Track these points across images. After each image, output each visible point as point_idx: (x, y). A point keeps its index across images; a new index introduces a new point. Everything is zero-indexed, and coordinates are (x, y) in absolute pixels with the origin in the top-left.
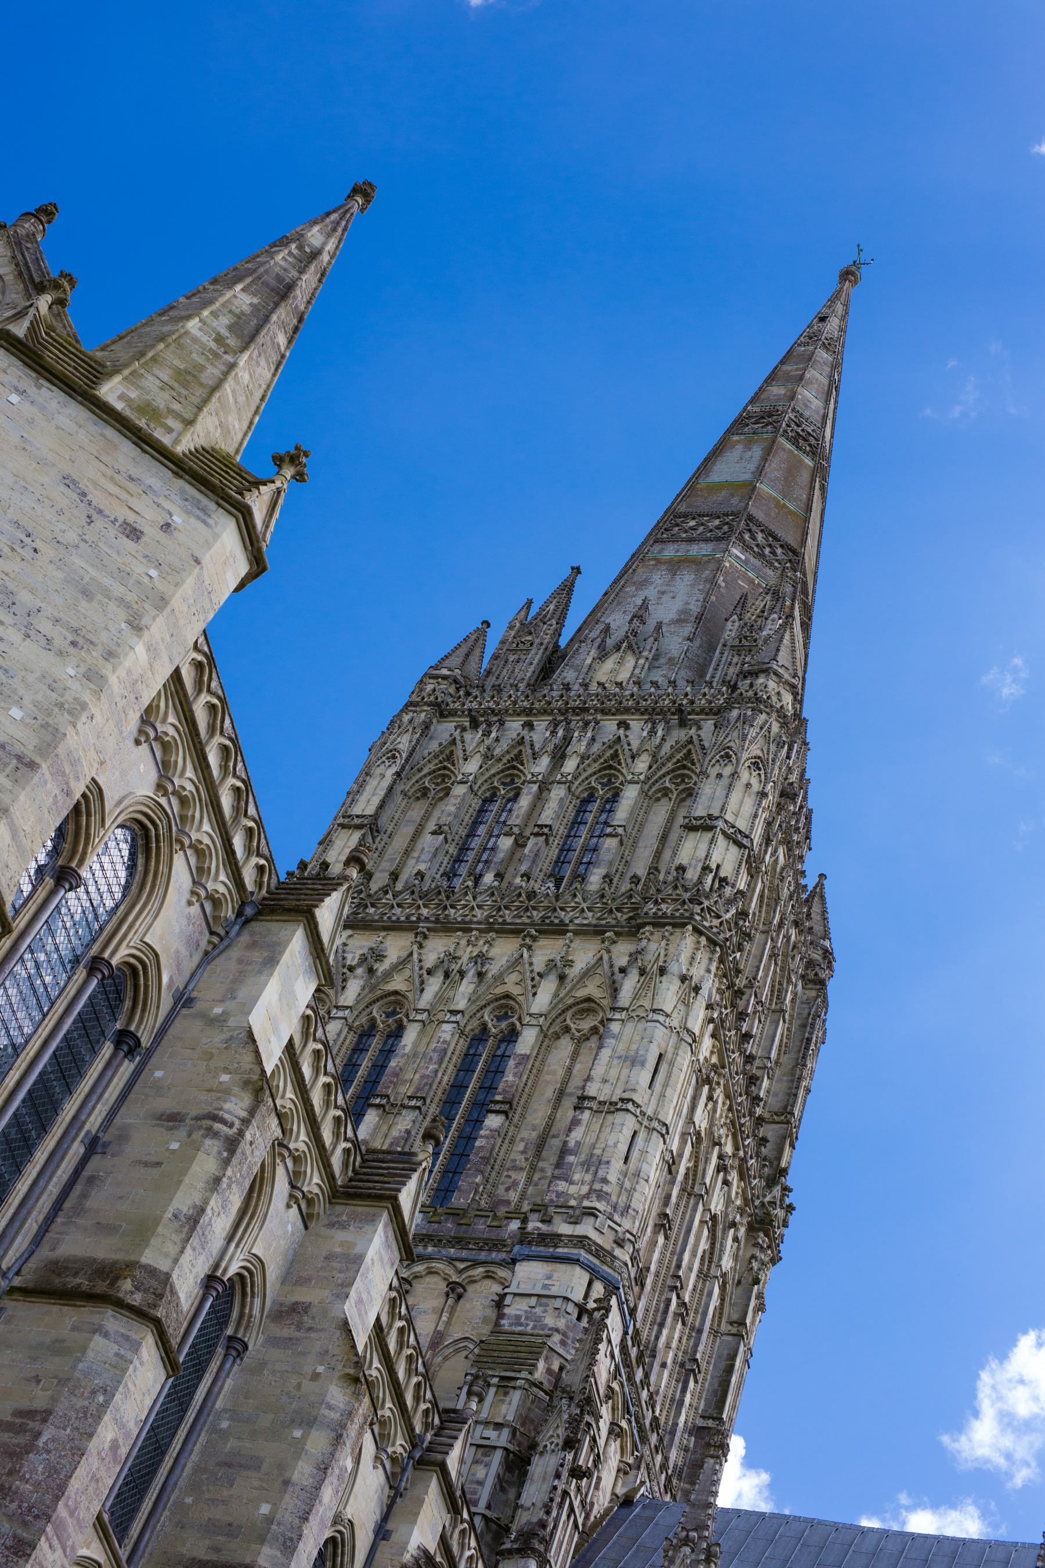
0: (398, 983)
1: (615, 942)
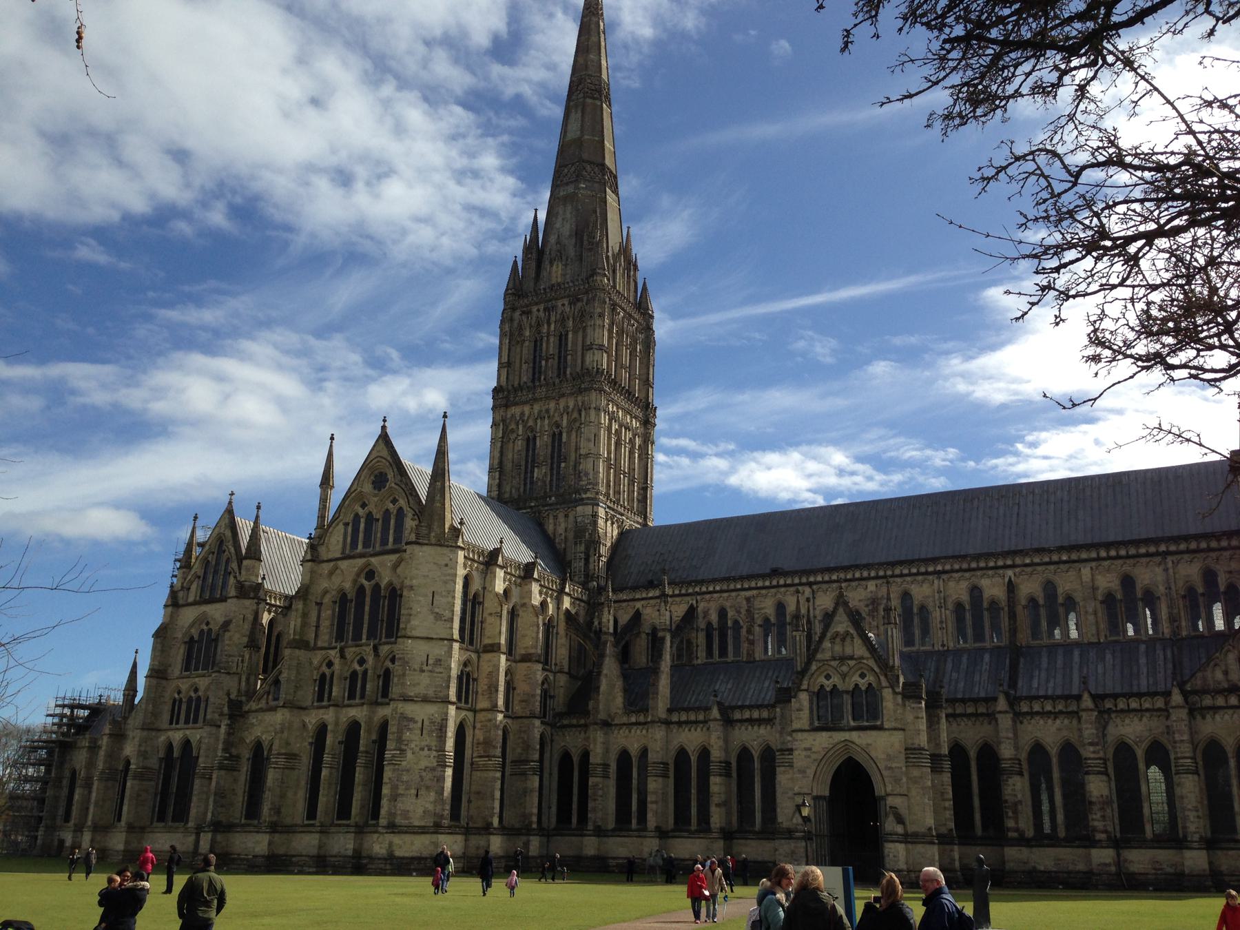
0: (531, 423)
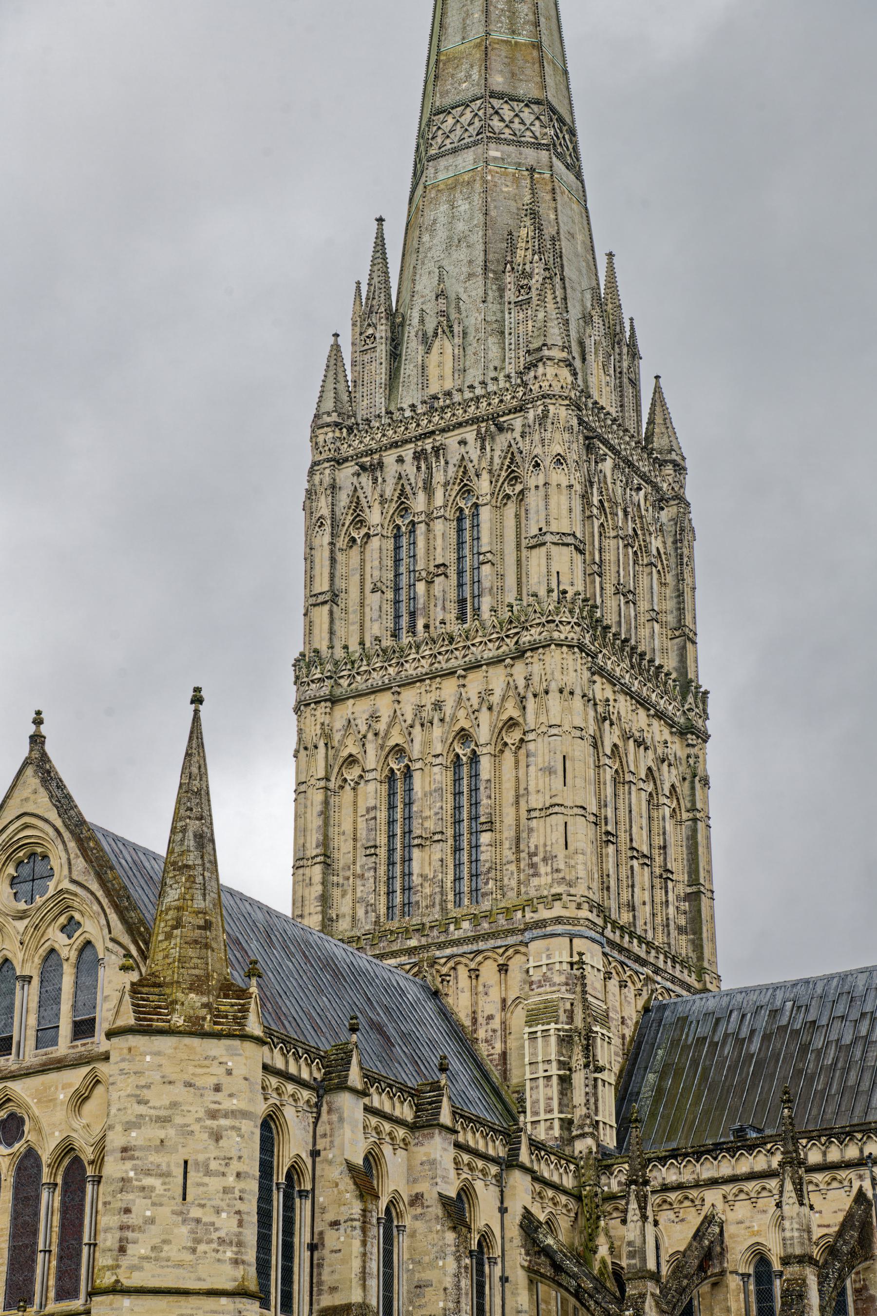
0: (396, 739)
1: (512, 665)
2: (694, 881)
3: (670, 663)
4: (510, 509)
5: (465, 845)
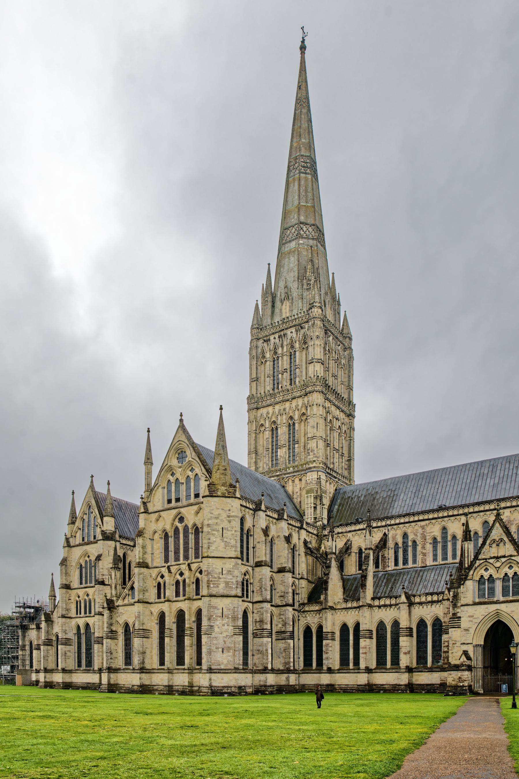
2: (349, 456)
3: (346, 396)
4: (304, 352)
5: (291, 448)
